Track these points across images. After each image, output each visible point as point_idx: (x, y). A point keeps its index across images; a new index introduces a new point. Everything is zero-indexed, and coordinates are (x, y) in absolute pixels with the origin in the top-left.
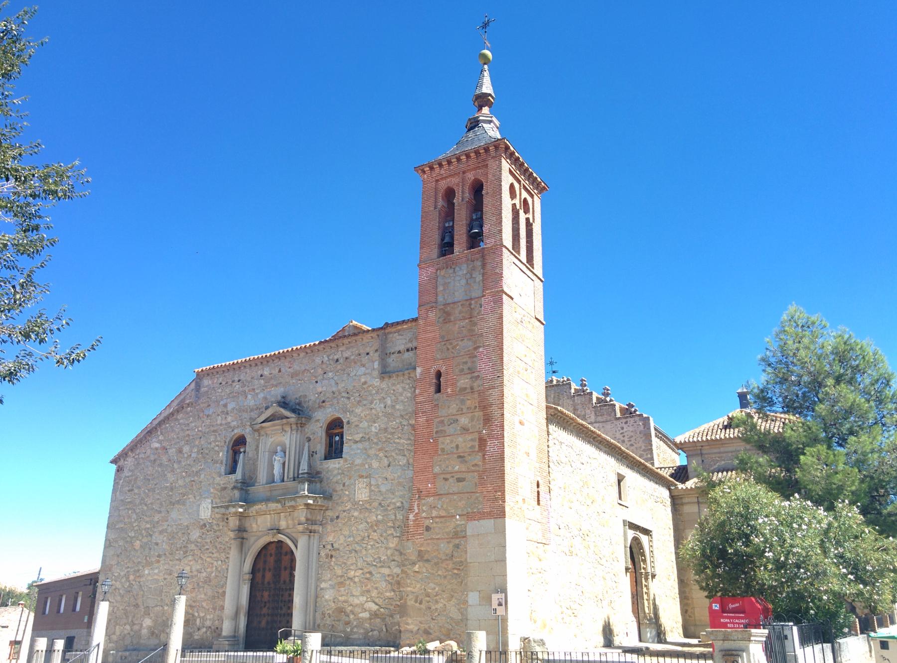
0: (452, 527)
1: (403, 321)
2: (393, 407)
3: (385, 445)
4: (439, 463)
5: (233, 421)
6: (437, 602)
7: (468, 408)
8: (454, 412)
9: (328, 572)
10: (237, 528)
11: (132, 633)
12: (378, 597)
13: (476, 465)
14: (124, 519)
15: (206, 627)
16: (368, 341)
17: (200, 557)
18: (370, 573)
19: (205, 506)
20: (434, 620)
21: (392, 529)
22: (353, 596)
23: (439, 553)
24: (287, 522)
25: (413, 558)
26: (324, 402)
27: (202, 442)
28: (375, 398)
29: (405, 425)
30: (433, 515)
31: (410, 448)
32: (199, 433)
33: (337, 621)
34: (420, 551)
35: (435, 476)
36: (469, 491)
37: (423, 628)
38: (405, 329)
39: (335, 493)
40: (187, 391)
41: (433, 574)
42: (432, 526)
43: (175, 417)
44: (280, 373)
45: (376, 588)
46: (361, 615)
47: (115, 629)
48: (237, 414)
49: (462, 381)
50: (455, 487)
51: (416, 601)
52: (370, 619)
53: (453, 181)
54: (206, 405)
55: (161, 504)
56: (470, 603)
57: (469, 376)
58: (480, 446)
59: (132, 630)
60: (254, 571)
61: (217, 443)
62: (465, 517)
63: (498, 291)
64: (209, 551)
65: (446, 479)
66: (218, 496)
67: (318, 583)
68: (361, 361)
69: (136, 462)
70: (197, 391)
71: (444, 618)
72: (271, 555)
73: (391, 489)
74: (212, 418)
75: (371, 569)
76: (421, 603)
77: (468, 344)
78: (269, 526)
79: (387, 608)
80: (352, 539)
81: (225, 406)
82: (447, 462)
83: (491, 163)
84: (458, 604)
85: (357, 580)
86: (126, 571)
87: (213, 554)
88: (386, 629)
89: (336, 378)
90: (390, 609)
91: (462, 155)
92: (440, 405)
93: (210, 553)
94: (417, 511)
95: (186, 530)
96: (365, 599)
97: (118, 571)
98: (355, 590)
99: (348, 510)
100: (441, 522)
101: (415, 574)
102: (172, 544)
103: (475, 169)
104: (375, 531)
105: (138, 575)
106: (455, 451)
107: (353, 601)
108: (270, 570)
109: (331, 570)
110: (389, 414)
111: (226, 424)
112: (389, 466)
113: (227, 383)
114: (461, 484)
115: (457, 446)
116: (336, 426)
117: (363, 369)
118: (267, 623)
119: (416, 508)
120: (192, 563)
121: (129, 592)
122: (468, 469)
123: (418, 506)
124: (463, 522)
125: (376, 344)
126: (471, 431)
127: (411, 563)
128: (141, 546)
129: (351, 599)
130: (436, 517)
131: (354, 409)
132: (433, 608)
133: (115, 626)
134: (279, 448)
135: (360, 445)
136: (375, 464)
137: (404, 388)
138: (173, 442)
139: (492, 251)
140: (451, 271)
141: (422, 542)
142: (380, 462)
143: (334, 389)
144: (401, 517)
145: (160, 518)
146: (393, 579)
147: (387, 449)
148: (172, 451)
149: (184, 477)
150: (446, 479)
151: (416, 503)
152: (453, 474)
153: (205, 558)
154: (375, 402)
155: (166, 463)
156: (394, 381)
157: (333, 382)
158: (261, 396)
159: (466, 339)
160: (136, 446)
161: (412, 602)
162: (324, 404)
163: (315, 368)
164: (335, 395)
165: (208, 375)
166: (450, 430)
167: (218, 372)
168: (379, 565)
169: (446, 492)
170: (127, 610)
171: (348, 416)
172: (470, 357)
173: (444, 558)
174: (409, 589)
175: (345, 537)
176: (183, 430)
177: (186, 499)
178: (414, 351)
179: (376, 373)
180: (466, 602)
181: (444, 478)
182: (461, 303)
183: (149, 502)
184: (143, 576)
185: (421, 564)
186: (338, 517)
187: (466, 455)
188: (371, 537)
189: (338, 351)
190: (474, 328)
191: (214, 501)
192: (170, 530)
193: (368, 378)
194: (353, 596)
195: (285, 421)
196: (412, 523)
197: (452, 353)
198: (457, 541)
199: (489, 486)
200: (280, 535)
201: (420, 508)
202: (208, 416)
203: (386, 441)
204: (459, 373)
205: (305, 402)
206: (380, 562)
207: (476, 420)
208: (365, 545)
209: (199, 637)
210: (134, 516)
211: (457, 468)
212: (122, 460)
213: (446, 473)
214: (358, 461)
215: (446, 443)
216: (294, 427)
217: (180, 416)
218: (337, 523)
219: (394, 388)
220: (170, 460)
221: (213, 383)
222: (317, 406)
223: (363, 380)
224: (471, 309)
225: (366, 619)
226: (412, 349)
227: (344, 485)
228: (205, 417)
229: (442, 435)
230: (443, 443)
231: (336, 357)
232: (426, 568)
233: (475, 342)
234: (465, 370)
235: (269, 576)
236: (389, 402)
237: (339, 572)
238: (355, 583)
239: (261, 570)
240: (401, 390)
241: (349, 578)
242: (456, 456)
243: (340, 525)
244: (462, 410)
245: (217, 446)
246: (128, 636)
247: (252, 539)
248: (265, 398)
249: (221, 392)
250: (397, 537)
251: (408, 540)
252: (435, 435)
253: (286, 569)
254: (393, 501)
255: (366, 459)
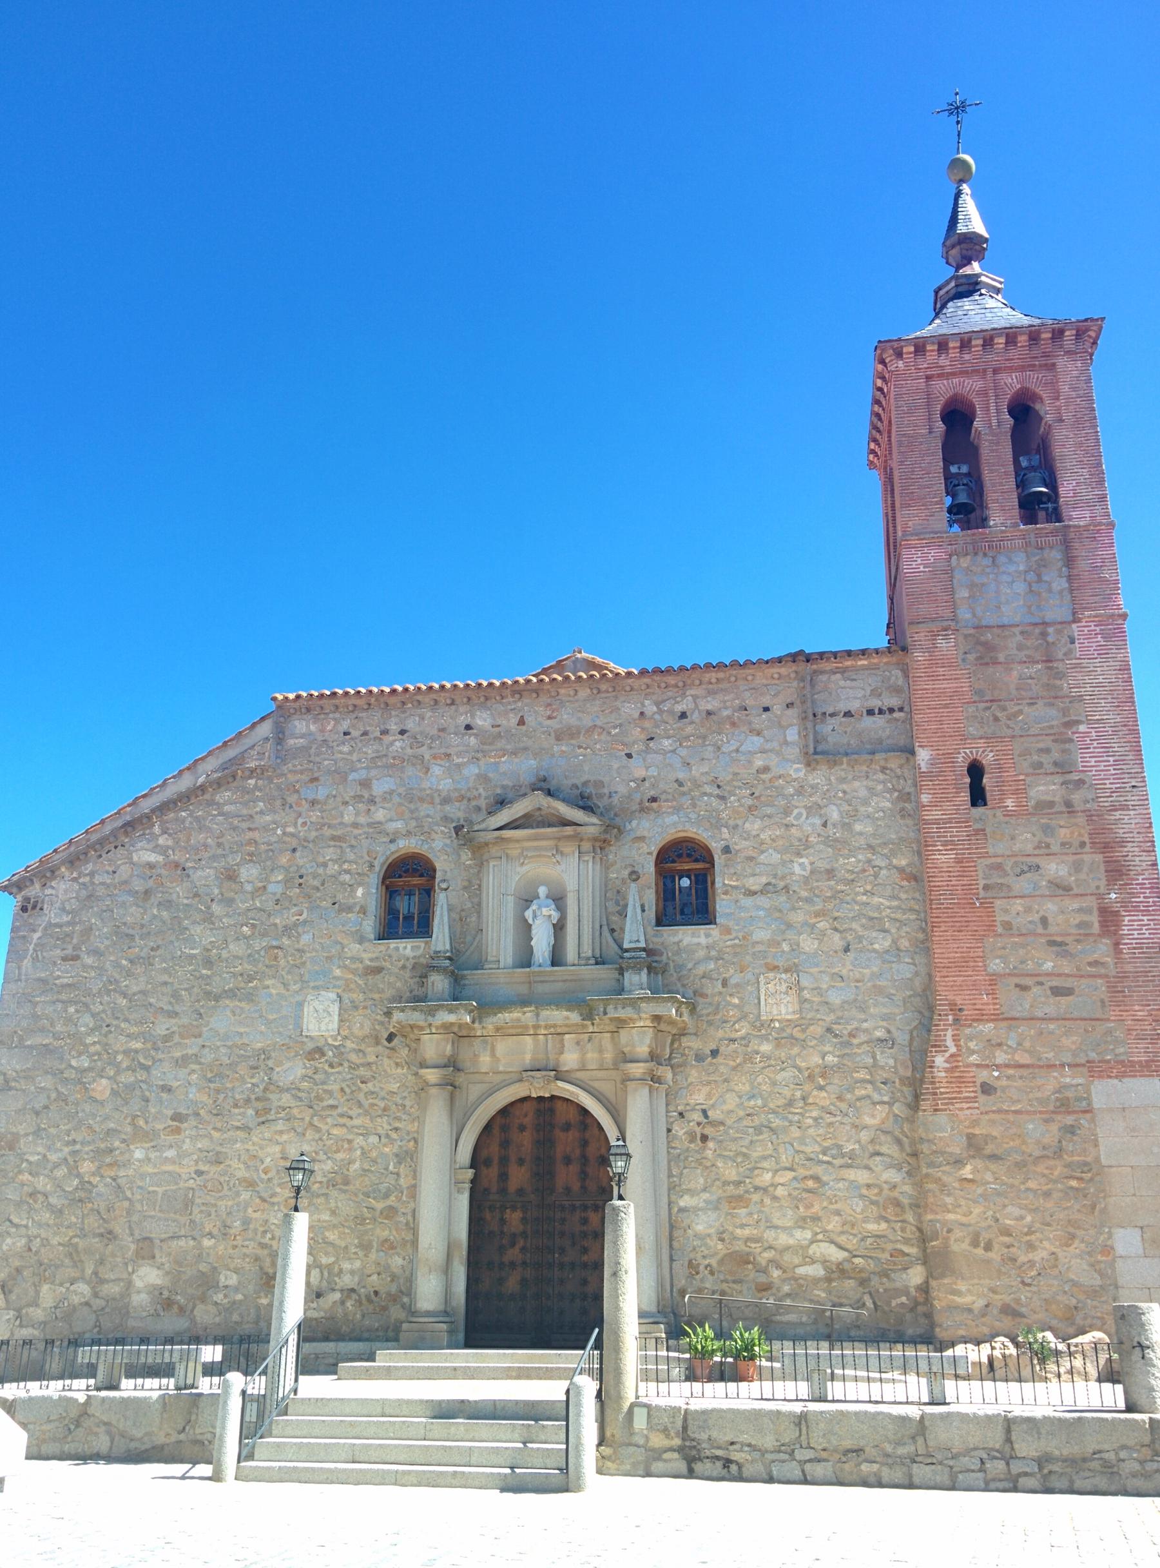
0: (1050, 1087)
1: (864, 652)
2: (847, 827)
3: (830, 906)
4: (999, 953)
5: (391, 820)
6: (1031, 1247)
7: (1063, 844)
8: (1029, 848)
9: (699, 1171)
10: (445, 1061)
11: (99, 1303)
12: (842, 1233)
13: (1095, 963)
14: (52, 1025)
15: (342, 1291)
16: (764, 681)
17: (311, 1124)
18: (816, 1178)
19: (320, 1008)
20: (1029, 1285)
21: (869, 1086)
22: (776, 1227)
23: (1024, 1142)
24: (583, 1054)
25: (957, 1148)
26: (654, 800)
27: (301, 862)
28: (793, 802)
29: (881, 868)
30: (999, 1061)
31: (899, 916)
32: (287, 839)
33: (734, 1282)
34: (970, 1137)
35: (994, 980)
36: (1084, 1015)
37: (999, 1304)
38: (857, 669)
39: (701, 1000)
40: (247, 742)
41: (1012, 1186)
42: (997, 1084)
43: (207, 796)
44: (524, 728)
45: (838, 1213)
46: (801, 1271)
47: (37, 1293)
48: (400, 804)
49: (1041, 788)
50: (1052, 1006)
51: (975, 1243)
52: (829, 1280)
53: (970, 386)
54: (307, 779)
55: (176, 995)
56: (1120, 1249)
57: (1058, 779)
58: (1104, 924)
59: (96, 1295)
60: (477, 1161)
61: (346, 866)
62: (1085, 1070)
63: (1113, 615)
64: (339, 1110)
65: (1024, 988)
66: (359, 986)
67: (673, 1198)
68: (750, 723)
69: (84, 893)
70: (278, 744)
71: (1056, 1283)
72: (522, 1128)
73: (855, 1000)
74: (328, 807)
75: (819, 1170)
76: (988, 1247)
77: (1044, 715)
78: (528, 1062)
79: (871, 1257)
80: (759, 1102)
81: (365, 784)
82: (1022, 952)
83: (1062, 362)
84: (1089, 1254)
85: (780, 1192)
86: (66, 1150)
87: (351, 1118)
88: (874, 1303)
89: (683, 752)
90: (879, 1259)
91: (1000, 335)
92: (988, 830)
93: (342, 1116)
94: (953, 1050)
95: (261, 1060)
96: (808, 1235)
97: (40, 1149)
98: (778, 1214)
99: (743, 1038)
100: (1021, 1078)
101: (966, 1185)
102: (218, 1091)
103: (1022, 369)
104: (821, 1088)
105: (108, 1160)
106: (1040, 930)
107: (776, 1239)
108: (521, 1161)
109: (707, 1168)
110: (836, 840)
111: (369, 825)
112: (847, 950)
113: (365, 734)
114: (1064, 1000)
115: (1044, 921)
116: (680, 856)
117: (757, 741)
118: (523, 1282)
119: (949, 1042)
120: (285, 1137)
121: (80, 1201)
122: (1078, 969)
123: (956, 1039)
124: (1080, 1081)
125: (790, 691)
126: (1076, 891)
127: (952, 1160)
128: (114, 1093)
129: (769, 1235)
130: (1007, 1066)
131: (740, 822)
132: (1023, 1258)
133: (36, 1287)
134: (542, 891)
135: (763, 901)
136: (808, 944)
137: (870, 789)
138: (206, 855)
139: (1085, 534)
140: (987, 561)
141: (974, 1117)
142: (821, 941)
143: (681, 776)
144: (891, 1062)
145: (175, 1029)
146: (879, 1194)
147: (837, 914)
148: (205, 875)
149: (245, 938)
150: (1024, 988)
151: (949, 1033)
152: (1040, 979)
153: (324, 1127)
154: (796, 812)
155: (185, 901)
156: (843, 774)
157: (676, 761)
158: (472, 771)
159: (1040, 703)
160: (86, 854)
161: (965, 1246)
162: (654, 805)
163: (621, 725)
164: (684, 789)
165: (308, 710)
166: (1022, 885)
167: (337, 707)
168: (837, 1162)
169: (1025, 1014)
170: (75, 1246)
171: (726, 836)
172: (1054, 741)
173: (1037, 1153)
174: (951, 1216)
175: (740, 1097)
176: (235, 829)
177: (255, 988)
178: (887, 716)
179: (794, 752)
180: (1108, 1250)
181: (1017, 986)
182: (1019, 629)
183: (135, 989)
184: (127, 1164)
185: (979, 1163)
186: (715, 1053)
187: (1068, 940)
188: (811, 1100)
189: (684, 695)
190: (1058, 682)
191: (345, 996)
192: (208, 1057)
193: (773, 761)
194: (776, 1227)
195: (569, 830)
196: (943, 1074)
197: (1008, 727)
198: (1069, 1120)
199: (1137, 1008)
200: (560, 1084)
201: (962, 1043)
202: (313, 803)
203: (834, 897)
204: (1031, 771)
205: (601, 796)
206: (843, 1156)
207: (1085, 869)
208: (796, 1118)
209: (322, 1314)
210: (87, 1019)
211: (1048, 966)
212: (37, 886)
213: (1022, 975)
214: (761, 935)
215: (1012, 910)
216: (586, 846)
217: (224, 796)
218: (711, 1064)
219: (845, 787)
220: (196, 895)
221: (322, 731)
222: (635, 807)
223: (759, 763)
224: (1047, 643)
225: (816, 1281)
226: (881, 712)
227: (725, 983)
228: (306, 805)
229: (1003, 894)
230: (1006, 911)
231: (679, 708)
232: (994, 1173)
233: (1065, 712)
234: (1046, 766)
235: (519, 1177)
236: (834, 814)
237: (731, 1173)
238: (775, 1198)
239: (496, 1161)
240: (863, 793)
241: (757, 1188)
242: (1043, 940)
243: (722, 1069)
244: (1048, 846)
245: (347, 872)
246: (85, 1308)
247: (475, 1091)
248: (483, 778)
249: (350, 753)
250: (884, 1103)
251: (936, 1110)
252: (982, 894)
253: (568, 1160)
254: (865, 1025)
255: (783, 932)
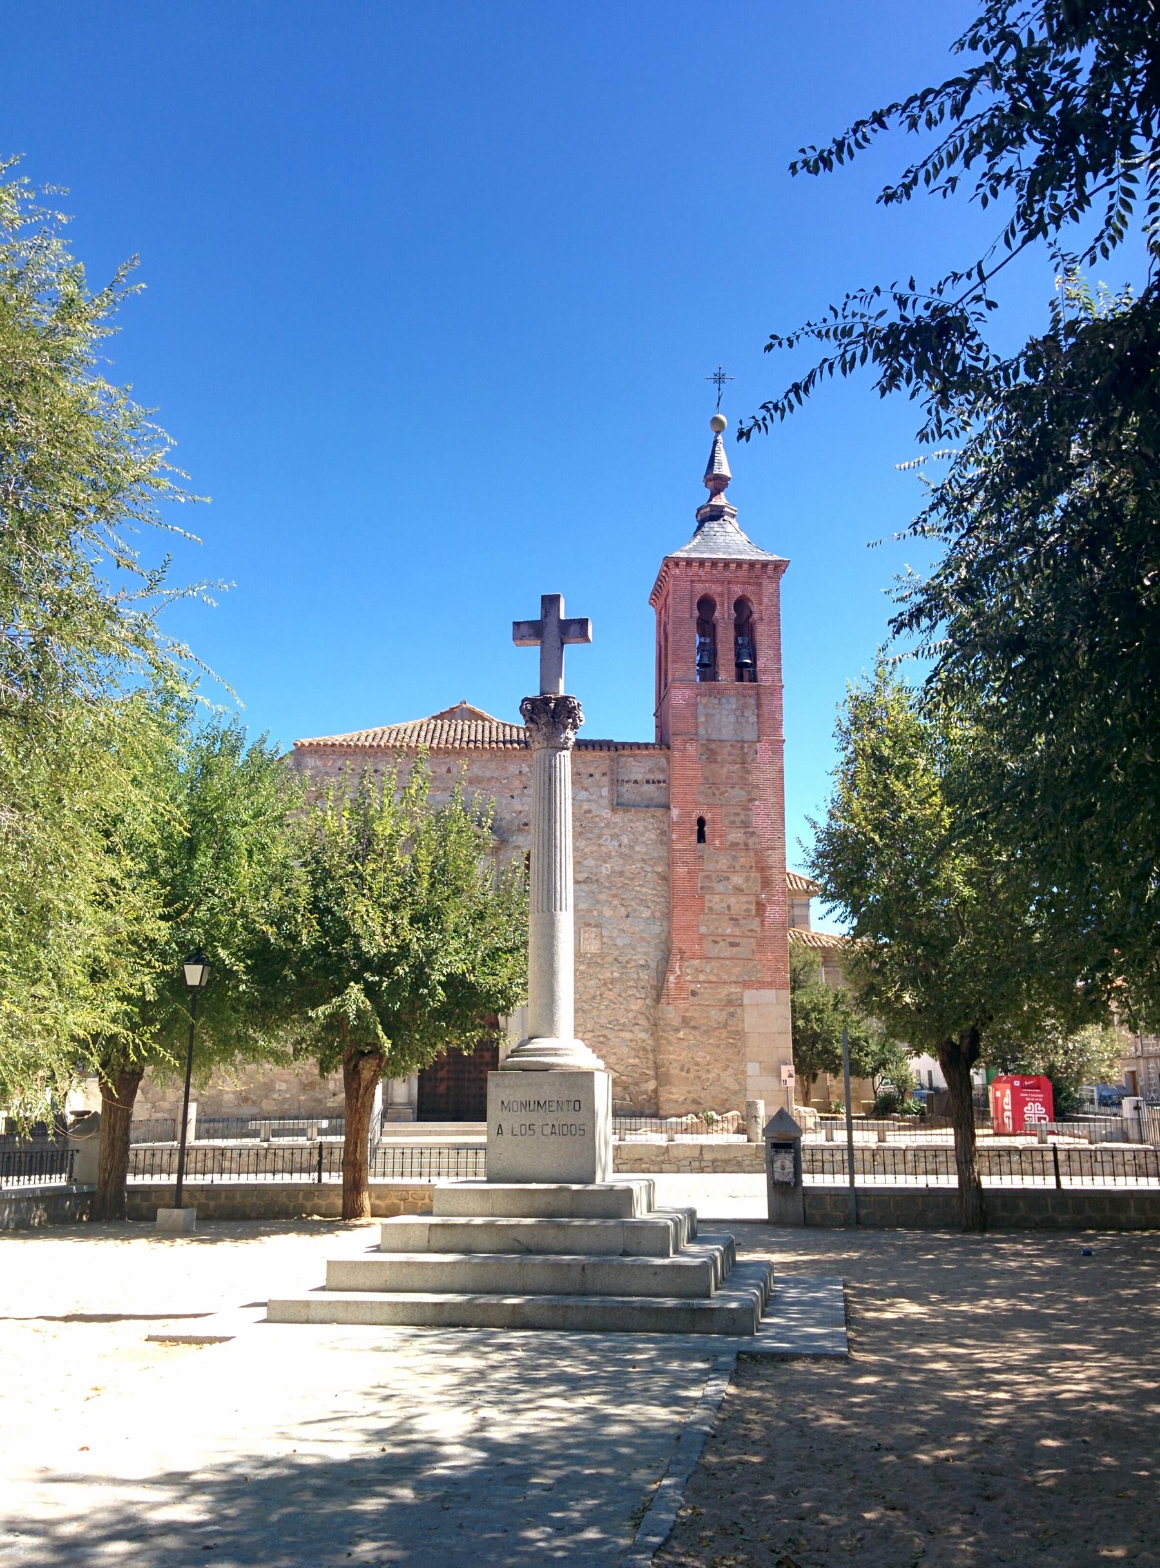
2: (632, 848)
6: (708, 1071)
8: (725, 868)
13: (752, 930)
25: (676, 1023)
26: (526, 824)
34: (684, 1017)
35: (702, 937)
45: (615, 1054)
50: (729, 952)
51: (682, 1070)
53: (715, 590)
56: (749, 1073)
57: (743, 830)
58: (757, 910)
65: (715, 942)
75: (606, 1032)
83: (765, 582)
94: (679, 973)
103: (744, 583)
104: (610, 990)
112: (628, 916)
115: (729, 907)
118: (448, 1088)
119: (677, 969)
123: (680, 968)
132: (704, 1077)
136: (608, 912)
137: (646, 828)
140: (716, 701)
150: (715, 942)
161: (677, 1071)
165: (316, 752)
166: (720, 887)
173: (715, 1026)
174: (672, 1057)
179: (605, 802)
180: (744, 1072)
185: (687, 1030)
193: (593, 807)
198: (732, 1009)
211: (729, 931)
215: (713, 901)
221: (325, 766)
222: (515, 828)
223: (586, 807)
226: (654, 782)
233: (749, 793)
236: (625, 840)
240: (641, 829)
